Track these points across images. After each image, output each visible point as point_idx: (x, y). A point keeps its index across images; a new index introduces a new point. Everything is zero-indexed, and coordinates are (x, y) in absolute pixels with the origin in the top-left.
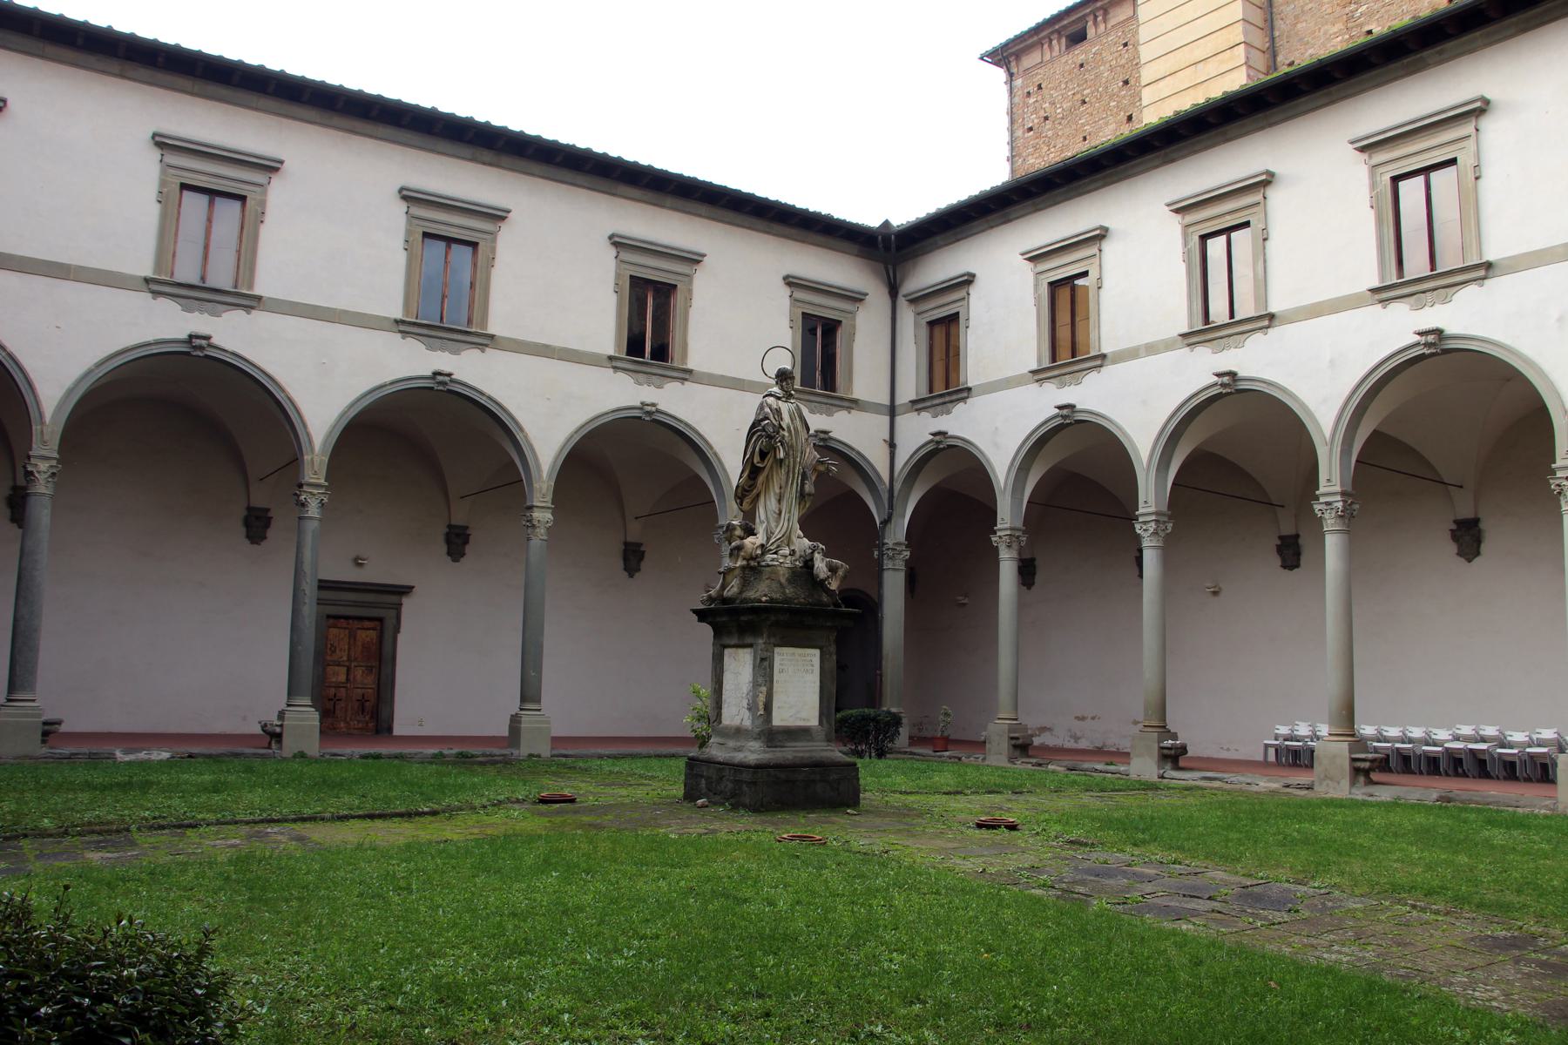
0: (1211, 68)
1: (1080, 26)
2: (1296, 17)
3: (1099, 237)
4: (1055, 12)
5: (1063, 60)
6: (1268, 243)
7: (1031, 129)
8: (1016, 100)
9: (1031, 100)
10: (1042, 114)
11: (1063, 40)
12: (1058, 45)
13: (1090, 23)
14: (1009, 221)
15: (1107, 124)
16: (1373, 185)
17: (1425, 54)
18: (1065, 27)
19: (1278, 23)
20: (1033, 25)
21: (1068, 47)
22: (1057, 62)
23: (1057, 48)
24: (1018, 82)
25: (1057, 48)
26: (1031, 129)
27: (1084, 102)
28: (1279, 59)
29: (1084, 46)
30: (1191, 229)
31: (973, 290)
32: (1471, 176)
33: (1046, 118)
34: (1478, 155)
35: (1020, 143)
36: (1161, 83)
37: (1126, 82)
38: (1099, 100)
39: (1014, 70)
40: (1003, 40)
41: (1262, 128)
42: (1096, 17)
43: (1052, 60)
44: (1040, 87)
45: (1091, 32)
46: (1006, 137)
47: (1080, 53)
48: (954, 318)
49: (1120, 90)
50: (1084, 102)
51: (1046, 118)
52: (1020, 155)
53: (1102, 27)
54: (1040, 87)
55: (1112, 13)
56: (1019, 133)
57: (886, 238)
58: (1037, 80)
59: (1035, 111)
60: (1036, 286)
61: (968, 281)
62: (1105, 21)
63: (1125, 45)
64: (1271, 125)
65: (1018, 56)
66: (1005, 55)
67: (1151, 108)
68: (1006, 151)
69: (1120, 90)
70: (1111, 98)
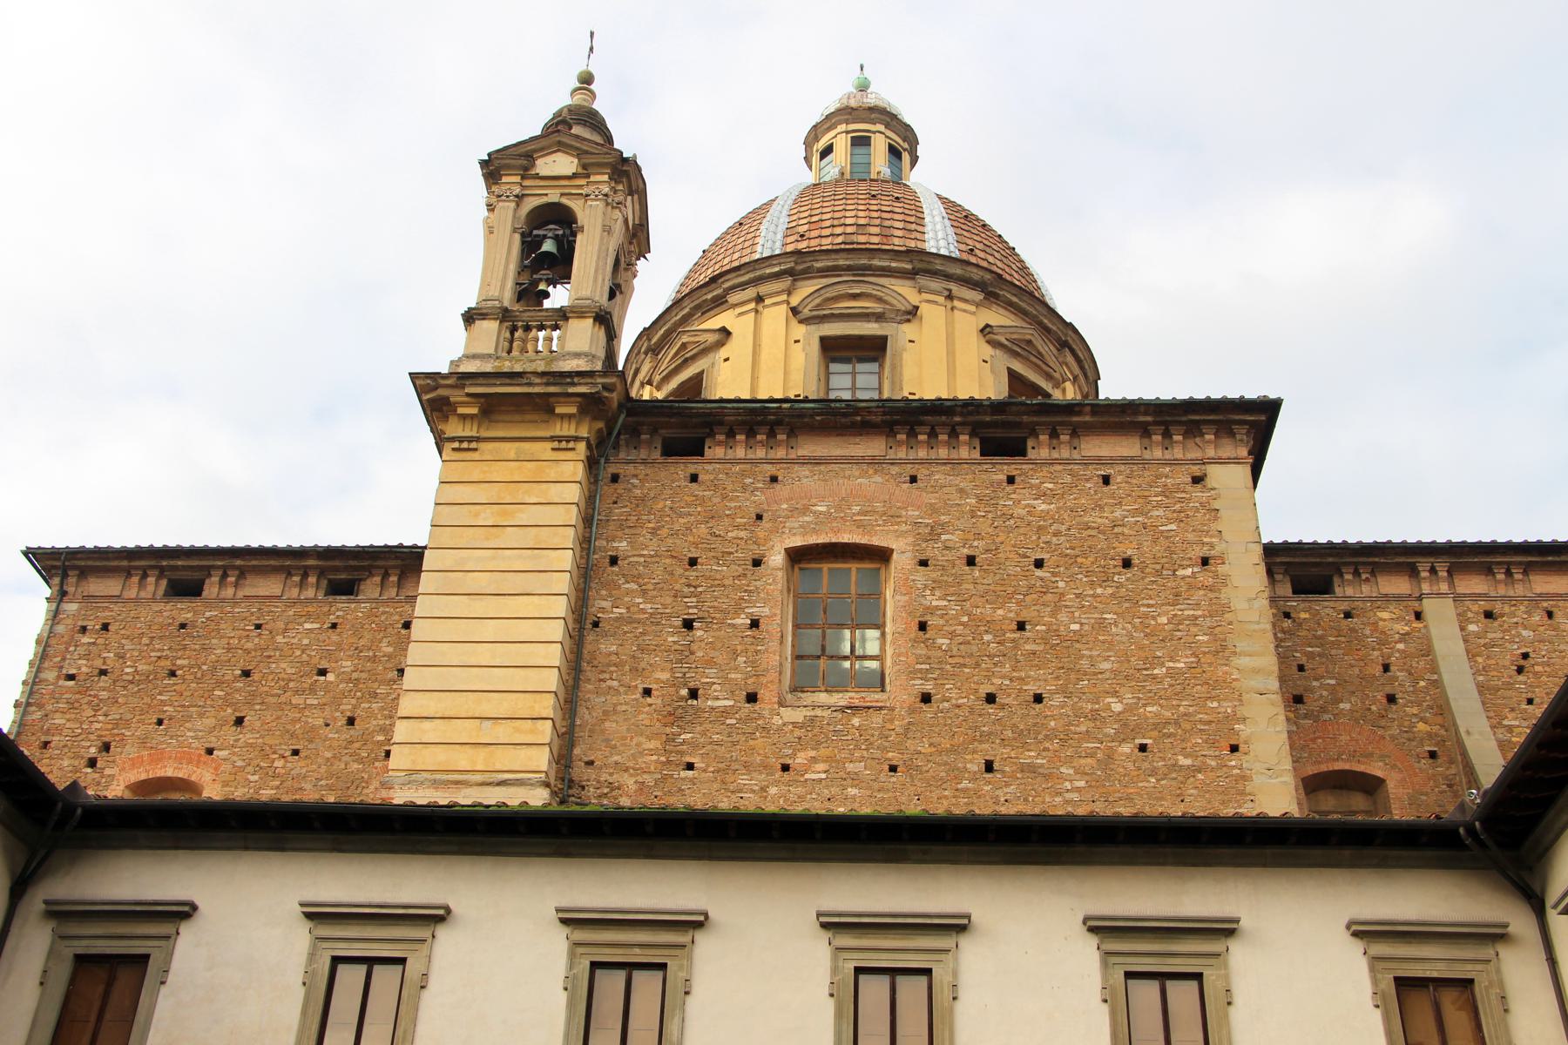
0: (502, 732)
1: (197, 575)
2: (605, 713)
3: (436, 917)
4: (172, 544)
5: (156, 607)
6: (689, 999)
7: (71, 677)
8: (60, 629)
9: (85, 640)
10: (99, 663)
11: (164, 583)
12: (154, 586)
13: (215, 579)
14: (282, 849)
15: (201, 715)
16: (835, 970)
17: (910, 847)
18: (176, 568)
19: (582, 711)
20: (131, 545)
21: (166, 594)
22: (148, 607)
23: (151, 588)
24: (71, 607)
25: (151, 588)
26: (71, 677)
27: (173, 674)
28: (577, 751)
29: (196, 603)
30: (581, 950)
31: (187, 932)
32: (948, 994)
33: (103, 672)
34: (955, 974)
35: (45, 689)
36: (427, 724)
37: (246, 674)
38: (198, 680)
39: (71, 589)
40: (75, 544)
41: (700, 858)
42: (225, 576)
43: (137, 600)
44: (105, 627)
45: (211, 589)
46: (22, 671)
47: (184, 609)
48: (140, 961)
49: (236, 679)
50: (173, 674)
51: (103, 672)
52: (40, 706)
53: (230, 592)
54: (105, 627)
55: (250, 580)
56: (50, 675)
57: (70, 809)
58: (104, 616)
59: (87, 656)
60: (312, 956)
61: (183, 912)
62: (236, 585)
63: (258, 627)
64: (711, 858)
65: (84, 573)
66: (58, 565)
67: (406, 749)
68: (16, 692)
69: (236, 679)
70: (219, 683)
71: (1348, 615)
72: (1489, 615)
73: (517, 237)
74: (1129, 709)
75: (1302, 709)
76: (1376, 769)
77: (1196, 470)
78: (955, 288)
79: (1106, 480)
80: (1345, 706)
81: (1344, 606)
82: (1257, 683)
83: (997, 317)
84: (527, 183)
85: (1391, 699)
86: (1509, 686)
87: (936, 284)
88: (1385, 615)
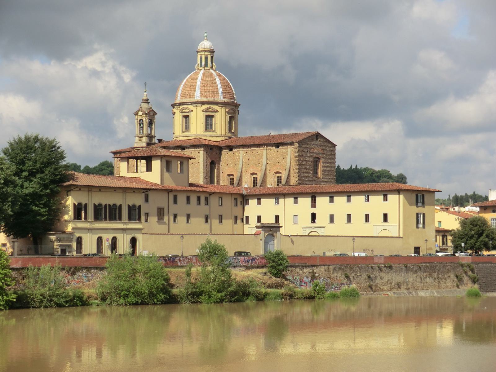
71: (233, 153)
72: (247, 153)
73: (138, 124)
74: (192, 180)
75: (228, 166)
76: (233, 173)
77: (199, 151)
78: (197, 105)
79: (191, 153)
80: (231, 166)
81: (233, 152)
82: (201, 177)
83: (205, 107)
84: (138, 116)
85: (236, 164)
86: (247, 162)
87: (195, 105)
88: (237, 153)
